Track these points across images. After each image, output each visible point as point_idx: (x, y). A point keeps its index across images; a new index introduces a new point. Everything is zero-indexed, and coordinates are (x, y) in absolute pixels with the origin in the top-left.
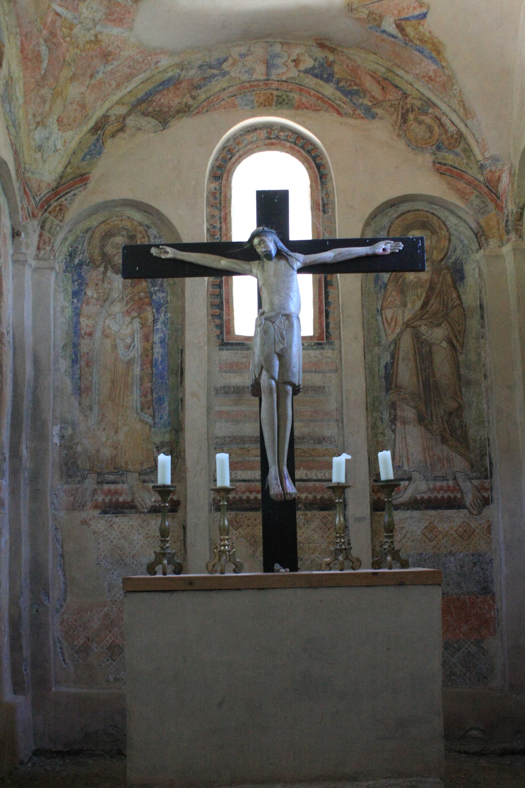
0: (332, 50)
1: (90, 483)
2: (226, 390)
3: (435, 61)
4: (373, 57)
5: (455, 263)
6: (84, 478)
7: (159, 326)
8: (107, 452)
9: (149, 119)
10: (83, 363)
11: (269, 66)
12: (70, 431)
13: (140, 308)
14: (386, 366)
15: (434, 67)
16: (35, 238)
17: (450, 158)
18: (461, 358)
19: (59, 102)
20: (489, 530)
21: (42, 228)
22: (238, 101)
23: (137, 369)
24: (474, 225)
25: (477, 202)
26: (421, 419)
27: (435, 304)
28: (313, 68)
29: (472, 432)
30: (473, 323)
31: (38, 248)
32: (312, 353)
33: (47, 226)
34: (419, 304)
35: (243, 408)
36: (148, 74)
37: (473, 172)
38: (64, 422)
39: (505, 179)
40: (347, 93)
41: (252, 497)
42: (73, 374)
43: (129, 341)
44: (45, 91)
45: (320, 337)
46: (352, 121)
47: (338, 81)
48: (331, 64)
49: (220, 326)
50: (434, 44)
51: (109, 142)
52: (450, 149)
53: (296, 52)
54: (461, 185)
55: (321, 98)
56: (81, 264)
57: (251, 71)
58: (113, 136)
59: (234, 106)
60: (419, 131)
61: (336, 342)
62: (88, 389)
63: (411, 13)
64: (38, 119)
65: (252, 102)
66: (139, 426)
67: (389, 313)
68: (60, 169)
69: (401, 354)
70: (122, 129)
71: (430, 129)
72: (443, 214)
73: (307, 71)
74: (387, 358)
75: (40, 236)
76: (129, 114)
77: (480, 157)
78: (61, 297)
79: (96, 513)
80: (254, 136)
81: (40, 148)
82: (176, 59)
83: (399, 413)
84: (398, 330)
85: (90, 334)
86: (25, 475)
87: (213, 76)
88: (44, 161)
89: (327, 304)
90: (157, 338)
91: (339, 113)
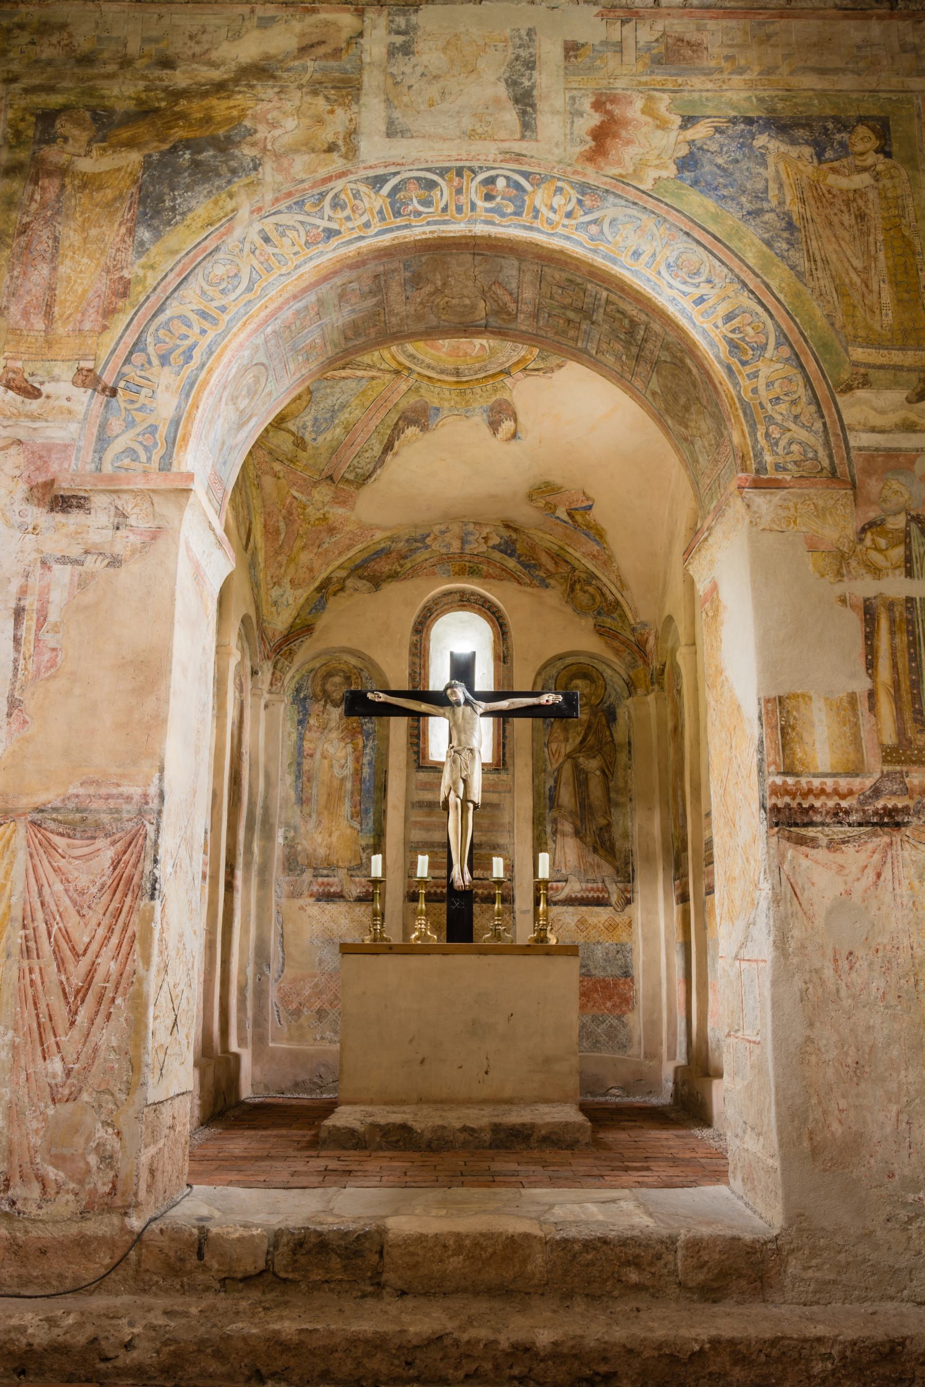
0: (516, 530)
1: (308, 876)
2: (421, 804)
3: (598, 544)
4: (548, 537)
5: (609, 707)
6: (303, 871)
7: (368, 750)
8: (322, 852)
9: (364, 582)
10: (305, 779)
11: (464, 541)
12: (292, 834)
13: (353, 735)
14: (550, 789)
15: (597, 548)
16: (268, 676)
17: (608, 621)
18: (611, 784)
19: (292, 566)
20: (630, 924)
21: (275, 667)
22: (437, 569)
23: (349, 785)
24: (625, 677)
25: (628, 658)
26: (577, 833)
27: (591, 740)
28: (500, 545)
29: (618, 844)
30: (622, 757)
31: (271, 684)
32: (491, 776)
33: (279, 666)
34: (579, 739)
35: (434, 819)
36: (364, 545)
37: (628, 634)
38: (288, 825)
39: (651, 641)
40: (526, 566)
41: (439, 891)
42: (297, 787)
43: (343, 761)
44: (282, 558)
45: (498, 764)
46: (529, 589)
47: (519, 556)
48: (514, 542)
49: (417, 753)
50: (597, 530)
51: (332, 600)
52: (609, 614)
53: (486, 531)
54: (616, 644)
55: (504, 569)
56: (305, 698)
57: (449, 545)
58: (335, 594)
59: (434, 574)
60: (584, 599)
61: (511, 768)
62: (309, 800)
63: (579, 505)
64: (275, 580)
65: (449, 571)
66: (349, 831)
67: (554, 746)
68: (290, 620)
69: (563, 780)
70: (342, 589)
71: (593, 598)
72: (601, 667)
73: (494, 547)
74: (550, 782)
75: (273, 674)
76: (348, 577)
77: (632, 622)
78: (289, 724)
79: (311, 900)
80: (450, 599)
81: (275, 603)
82: (388, 534)
83: (559, 827)
84: (561, 760)
85: (311, 756)
86: (255, 868)
87: (419, 548)
88: (279, 614)
89: (504, 737)
90: (366, 760)
91: (520, 583)
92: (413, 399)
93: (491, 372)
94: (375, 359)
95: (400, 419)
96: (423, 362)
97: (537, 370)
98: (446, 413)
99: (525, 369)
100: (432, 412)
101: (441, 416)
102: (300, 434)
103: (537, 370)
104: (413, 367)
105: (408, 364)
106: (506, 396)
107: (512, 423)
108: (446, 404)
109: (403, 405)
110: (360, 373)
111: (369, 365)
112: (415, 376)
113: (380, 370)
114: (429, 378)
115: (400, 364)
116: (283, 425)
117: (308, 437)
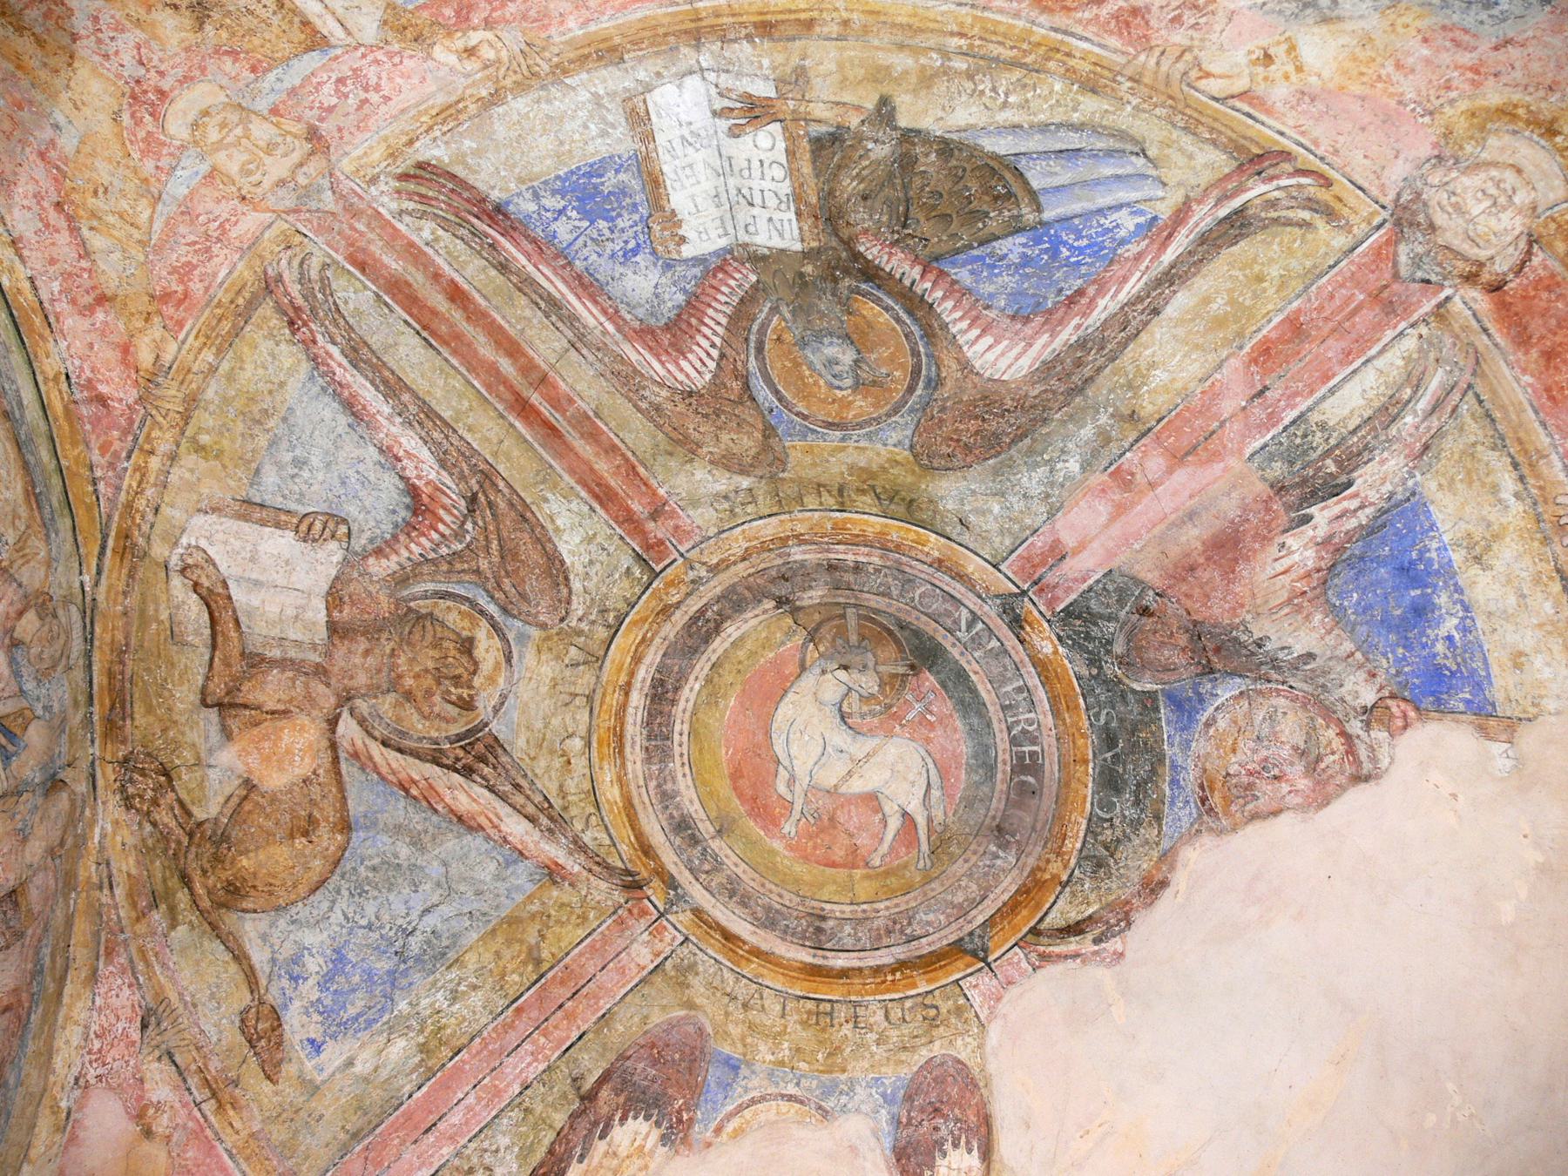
92: (660, 1012)
93: (925, 947)
94: (571, 785)
95: (604, 1078)
96: (718, 866)
97: (1074, 929)
98: (756, 1084)
99: (1035, 931)
100: (714, 1074)
101: (738, 1096)
102: (273, 996)
103: (1074, 929)
104: (684, 877)
105: (669, 859)
106: (963, 1049)
107: (974, 1160)
108: (764, 1053)
109: (626, 1028)
110: (516, 827)
111: (546, 807)
112: (683, 918)
113: (579, 846)
114: (728, 936)
115: (646, 850)
116: (230, 919)
117: (298, 1025)
